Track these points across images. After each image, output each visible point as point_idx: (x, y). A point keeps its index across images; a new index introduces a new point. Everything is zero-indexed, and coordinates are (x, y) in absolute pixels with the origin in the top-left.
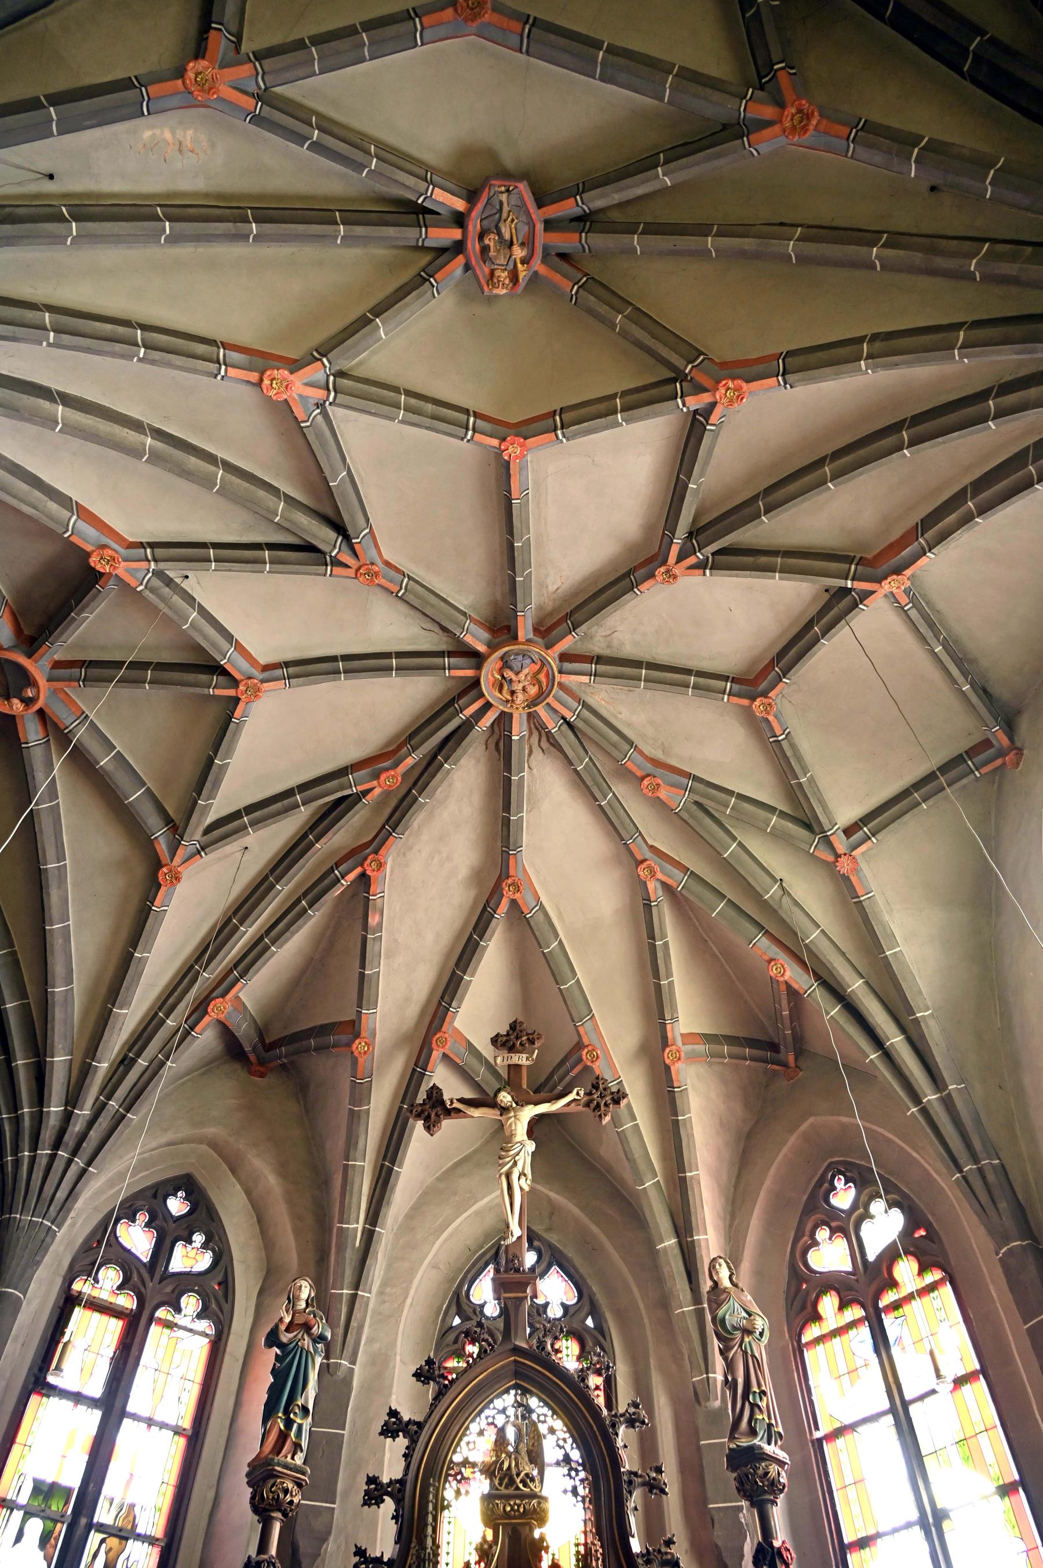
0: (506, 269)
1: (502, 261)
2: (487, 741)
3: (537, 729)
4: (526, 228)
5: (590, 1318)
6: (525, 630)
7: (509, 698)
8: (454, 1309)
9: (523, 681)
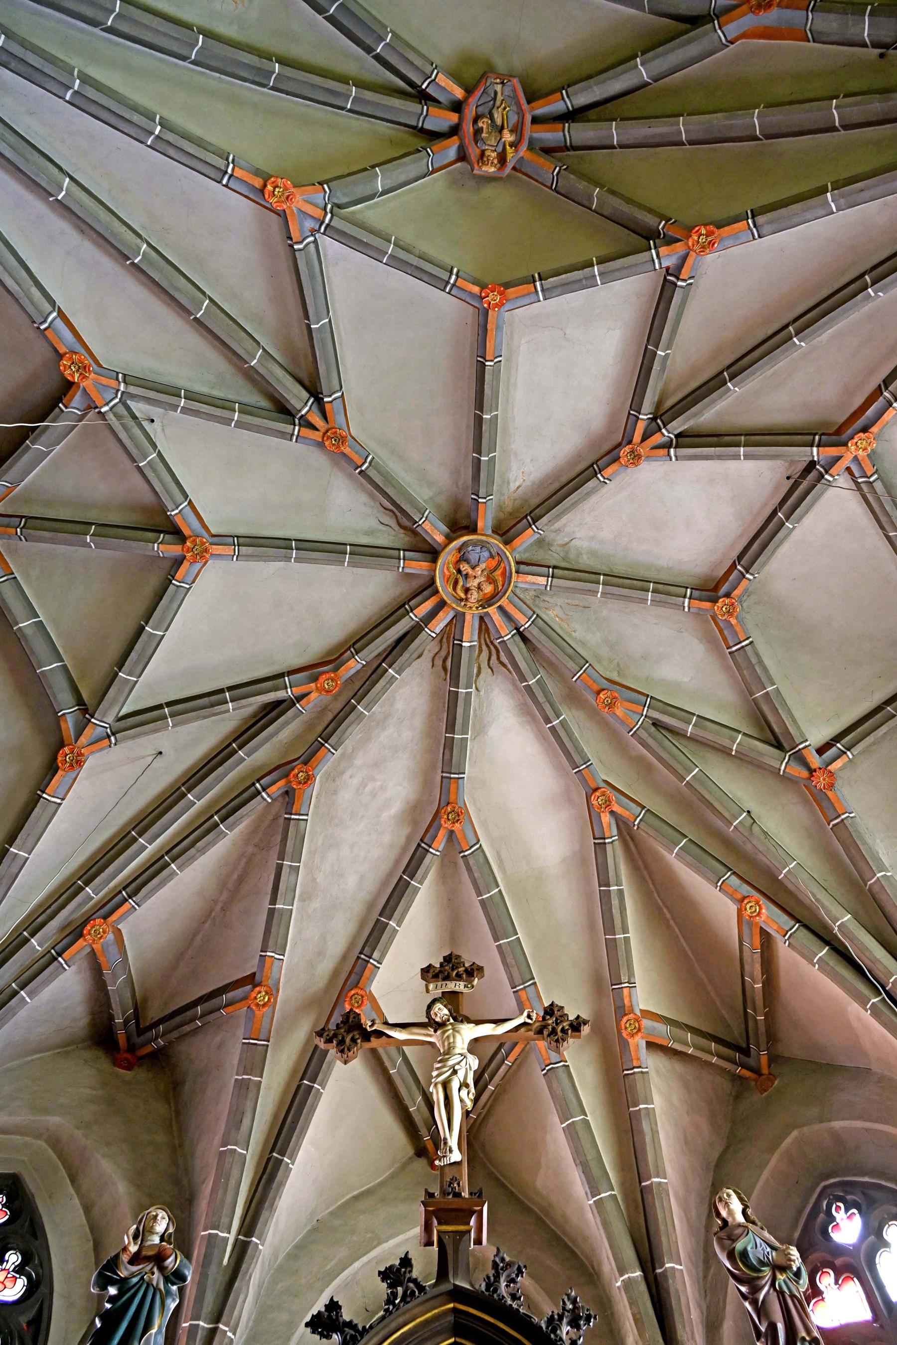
0: (495, 150)
1: (493, 142)
2: (435, 656)
3: (487, 646)
4: (516, 117)
6: (485, 522)
7: (463, 595)
9: (477, 578)
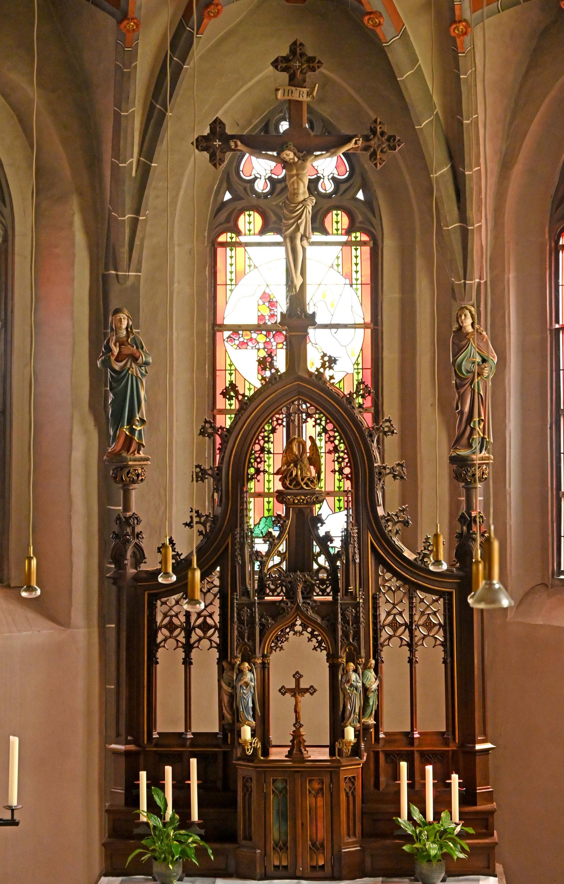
5: (361, 191)
8: (225, 185)
